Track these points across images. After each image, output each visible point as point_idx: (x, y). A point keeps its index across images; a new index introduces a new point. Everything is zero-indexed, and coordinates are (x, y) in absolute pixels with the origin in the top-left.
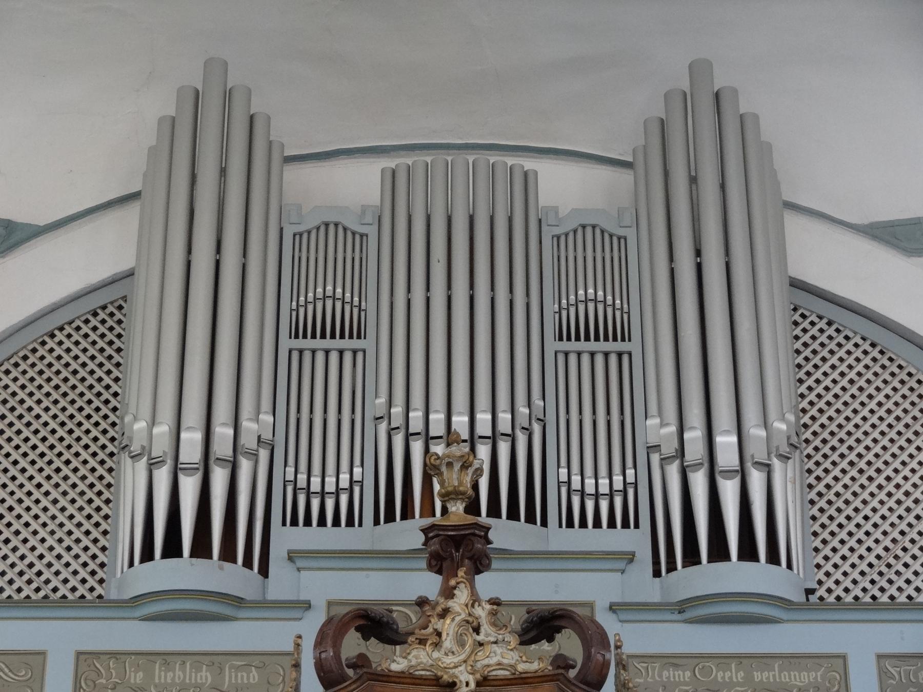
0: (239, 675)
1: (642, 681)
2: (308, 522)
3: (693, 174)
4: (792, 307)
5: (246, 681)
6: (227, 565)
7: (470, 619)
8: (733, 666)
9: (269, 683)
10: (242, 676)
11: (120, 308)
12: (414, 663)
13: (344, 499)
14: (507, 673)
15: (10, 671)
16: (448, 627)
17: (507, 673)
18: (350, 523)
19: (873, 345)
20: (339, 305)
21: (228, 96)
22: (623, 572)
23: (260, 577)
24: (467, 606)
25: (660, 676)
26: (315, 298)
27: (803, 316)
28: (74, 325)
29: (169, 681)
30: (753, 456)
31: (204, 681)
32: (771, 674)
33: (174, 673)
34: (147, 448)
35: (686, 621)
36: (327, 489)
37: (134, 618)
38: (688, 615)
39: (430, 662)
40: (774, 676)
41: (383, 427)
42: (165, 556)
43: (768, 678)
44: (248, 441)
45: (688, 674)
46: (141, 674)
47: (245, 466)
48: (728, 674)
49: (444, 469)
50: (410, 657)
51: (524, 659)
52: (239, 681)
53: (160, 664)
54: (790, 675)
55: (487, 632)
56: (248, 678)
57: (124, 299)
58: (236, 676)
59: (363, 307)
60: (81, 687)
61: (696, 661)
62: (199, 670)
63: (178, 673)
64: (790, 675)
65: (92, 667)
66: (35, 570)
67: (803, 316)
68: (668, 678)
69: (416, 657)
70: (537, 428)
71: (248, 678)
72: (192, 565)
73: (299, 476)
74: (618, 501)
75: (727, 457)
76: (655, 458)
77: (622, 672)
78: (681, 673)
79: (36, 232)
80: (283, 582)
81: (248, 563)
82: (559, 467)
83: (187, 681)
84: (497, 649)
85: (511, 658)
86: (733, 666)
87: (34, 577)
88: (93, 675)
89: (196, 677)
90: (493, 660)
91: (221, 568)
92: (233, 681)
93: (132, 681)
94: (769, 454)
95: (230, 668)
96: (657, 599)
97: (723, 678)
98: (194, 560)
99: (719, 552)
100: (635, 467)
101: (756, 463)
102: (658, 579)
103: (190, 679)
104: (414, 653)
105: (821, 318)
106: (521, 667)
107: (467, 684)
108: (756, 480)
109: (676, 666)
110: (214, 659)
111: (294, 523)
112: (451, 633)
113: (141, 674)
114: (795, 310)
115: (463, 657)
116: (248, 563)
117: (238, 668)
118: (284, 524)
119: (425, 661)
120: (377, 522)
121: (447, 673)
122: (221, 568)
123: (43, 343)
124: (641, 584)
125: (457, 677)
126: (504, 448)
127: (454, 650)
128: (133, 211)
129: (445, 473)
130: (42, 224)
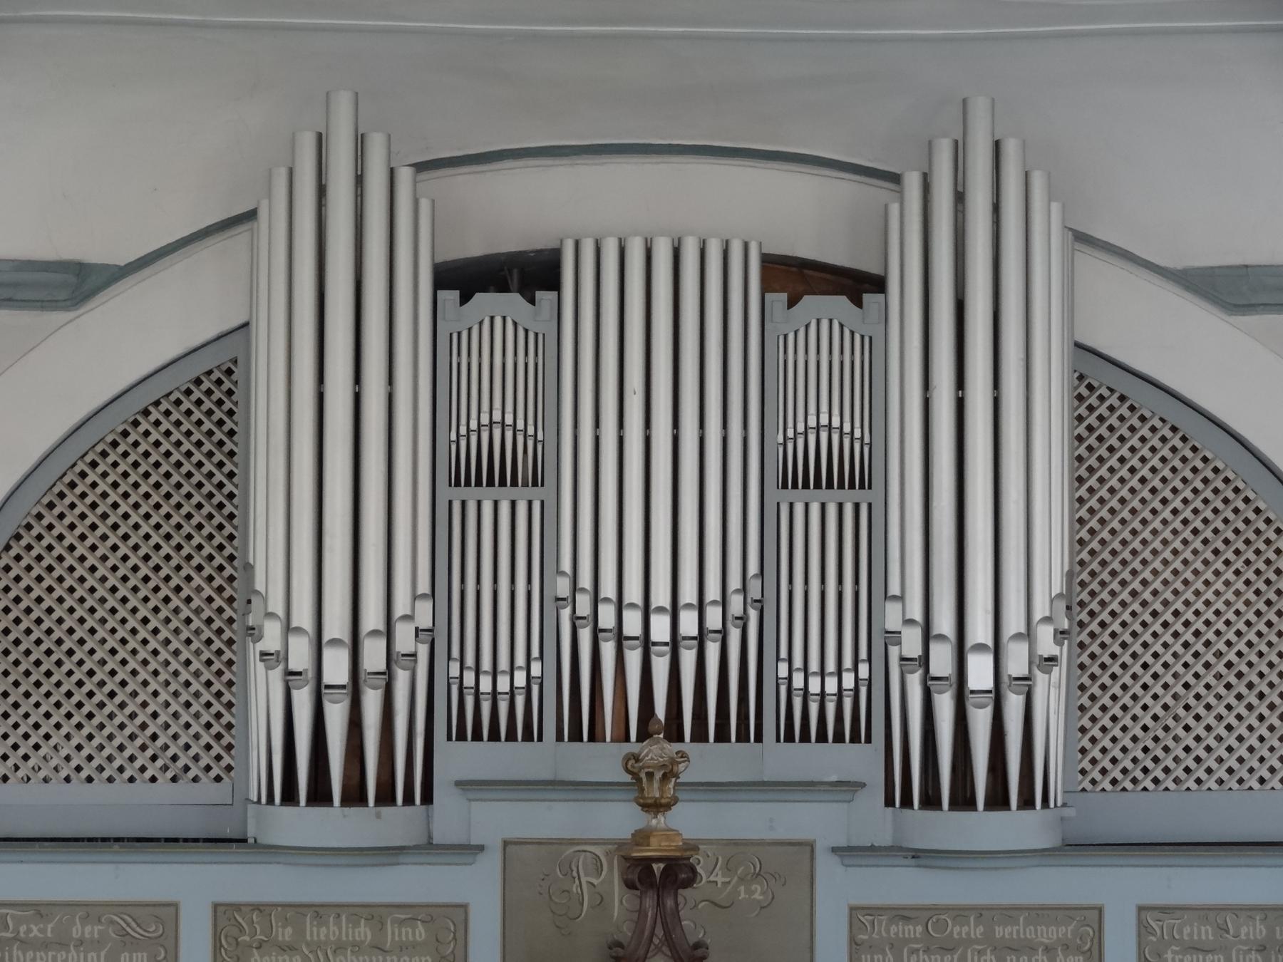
1: (866, 937)
2: (477, 736)
3: (960, 189)
4: (1076, 375)
5: (411, 938)
6: (386, 810)
10: (407, 933)
11: (229, 372)
15: (138, 925)
18: (528, 737)
19: (1174, 429)
20: (509, 434)
21: (360, 144)
25: (888, 931)
26: (479, 425)
27: (1090, 388)
28: (173, 398)
29: (322, 938)
32: (1015, 928)
33: (328, 928)
34: (281, 656)
35: (919, 866)
36: (499, 689)
38: (922, 862)
40: (1018, 932)
41: (566, 613)
43: (1011, 934)
44: (405, 639)
45: (919, 928)
46: (289, 930)
47: (402, 678)
48: (965, 929)
54: (1036, 931)
56: (414, 934)
57: (235, 362)
58: (400, 935)
59: (540, 437)
60: (221, 946)
62: (356, 924)
64: (1036, 931)
65: (233, 922)
66: (149, 732)
67: (1090, 388)
68: (897, 934)
70: (753, 615)
71: (414, 934)
73: (465, 673)
75: (980, 673)
76: (894, 652)
78: (911, 927)
79: (116, 274)
80: (451, 815)
81: (409, 799)
82: (778, 659)
87: (148, 742)
88: (235, 931)
91: (378, 816)
94: (1030, 663)
95: (392, 923)
96: (885, 839)
97: (960, 933)
98: (346, 809)
99: (963, 800)
100: (869, 659)
102: (890, 809)
103: (347, 936)
105: (1112, 390)
108: (1014, 705)
110: (374, 913)
113: (289, 930)
114: (1081, 378)
116: (409, 799)
117: (402, 923)
118: (449, 738)
120: (560, 737)
122: (378, 816)
123: (136, 424)
124: (872, 820)
126: (713, 650)
128: (238, 239)
129: (644, 780)
130: (122, 264)
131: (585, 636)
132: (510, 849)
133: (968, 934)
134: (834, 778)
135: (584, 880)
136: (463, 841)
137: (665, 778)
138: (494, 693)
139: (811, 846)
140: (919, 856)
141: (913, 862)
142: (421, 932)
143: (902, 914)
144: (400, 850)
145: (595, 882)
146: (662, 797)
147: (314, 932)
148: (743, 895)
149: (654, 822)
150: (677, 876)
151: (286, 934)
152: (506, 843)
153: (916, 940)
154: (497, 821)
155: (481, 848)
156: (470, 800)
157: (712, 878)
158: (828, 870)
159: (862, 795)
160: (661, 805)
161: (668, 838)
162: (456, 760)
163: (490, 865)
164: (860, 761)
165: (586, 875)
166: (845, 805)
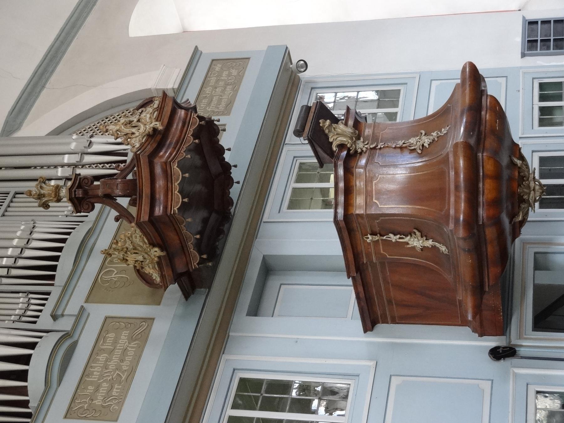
17: (156, 113)
30: (85, 147)
37: (57, 389)
42: (26, 380)
46: (89, 387)
49: (42, 192)
53: (88, 377)
58: (110, 343)
60: (85, 417)
62: (98, 360)
65: (76, 411)
88: (81, 410)
93: (92, 391)
101: (89, 146)
113: (89, 387)
129: (44, 192)
131: (14, 272)
135: (113, 276)
142: (112, 335)
145: (116, 272)
147: (94, 378)
151: (91, 388)
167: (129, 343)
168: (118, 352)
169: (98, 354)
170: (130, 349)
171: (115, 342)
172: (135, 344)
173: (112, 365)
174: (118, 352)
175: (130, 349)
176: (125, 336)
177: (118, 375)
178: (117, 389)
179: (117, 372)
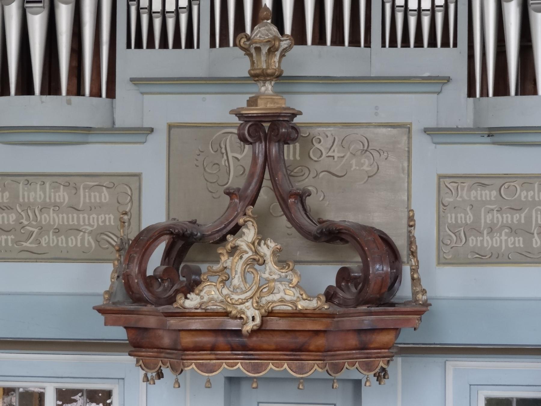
0: (92, 194)
1: (451, 200)
2: (151, 45)
5: (98, 201)
6: (75, 99)
7: (257, 257)
8: (536, 185)
9: (118, 202)
10: (95, 196)
12: (205, 300)
13: (183, 18)
14: (290, 308)
16: (236, 265)
18: (190, 45)
22: (439, 93)
23: (109, 100)
24: (253, 243)
31: (62, 201)
33: (36, 192)
35: (494, 143)
36: (168, 9)
38: (495, 139)
39: (221, 298)
45: (494, 193)
46: (7, 194)
48: (531, 193)
50: (202, 294)
51: (304, 296)
52: (93, 201)
55: (271, 270)
58: (90, 197)
61: (502, 181)
63: (39, 192)
69: (209, 293)
72: (42, 102)
74: (439, 17)
77: (411, 257)
78: (487, 192)
80: (129, 105)
83: (48, 200)
84: (280, 286)
85: (291, 294)
86: (536, 185)
89: (55, 196)
90: (276, 297)
91: (69, 103)
92: (87, 201)
95: (84, 188)
96: (468, 122)
97: (526, 197)
98: (44, 97)
102: (471, 99)
103: (50, 198)
104: (206, 289)
106: (301, 305)
107: (253, 319)
109: (484, 185)
111: (139, 45)
112: (239, 271)
113: (7, 194)
115: (249, 294)
118: (129, 46)
119: (216, 297)
120: (213, 45)
121: (236, 308)
122: (69, 103)
124: (456, 106)
125: (244, 313)
127: (242, 286)
129: (254, 55)
132: (173, 131)
133: (533, 197)
134: (427, 74)
135: (230, 155)
136: (140, 126)
137: (271, 51)
138: (164, 13)
139: (407, 128)
140: (494, 134)
141: (489, 140)
142: (105, 196)
143: (480, 181)
144: (88, 130)
145: (239, 156)
146: (268, 68)
148: (354, 167)
149: (263, 89)
150: (278, 129)
152: (170, 127)
153: (490, 202)
154: (163, 110)
155: (152, 130)
156: (142, 93)
157: (330, 154)
158: (421, 144)
159: (448, 88)
160: (268, 75)
161: (273, 101)
162: (132, 63)
163: (158, 142)
164: (450, 61)
165: (232, 152)
166: (436, 95)
167: (90, 233)
168: (72, 219)
169: (67, 185)
170: (79, 238)
171: (91, 208)
172: (89, 242)
173: (51, 218)
174: (72, 219)
175: (79, 238)
176: (104, 222)
177: (32, 233)
178: (6, 240)
179: (36, 230)
